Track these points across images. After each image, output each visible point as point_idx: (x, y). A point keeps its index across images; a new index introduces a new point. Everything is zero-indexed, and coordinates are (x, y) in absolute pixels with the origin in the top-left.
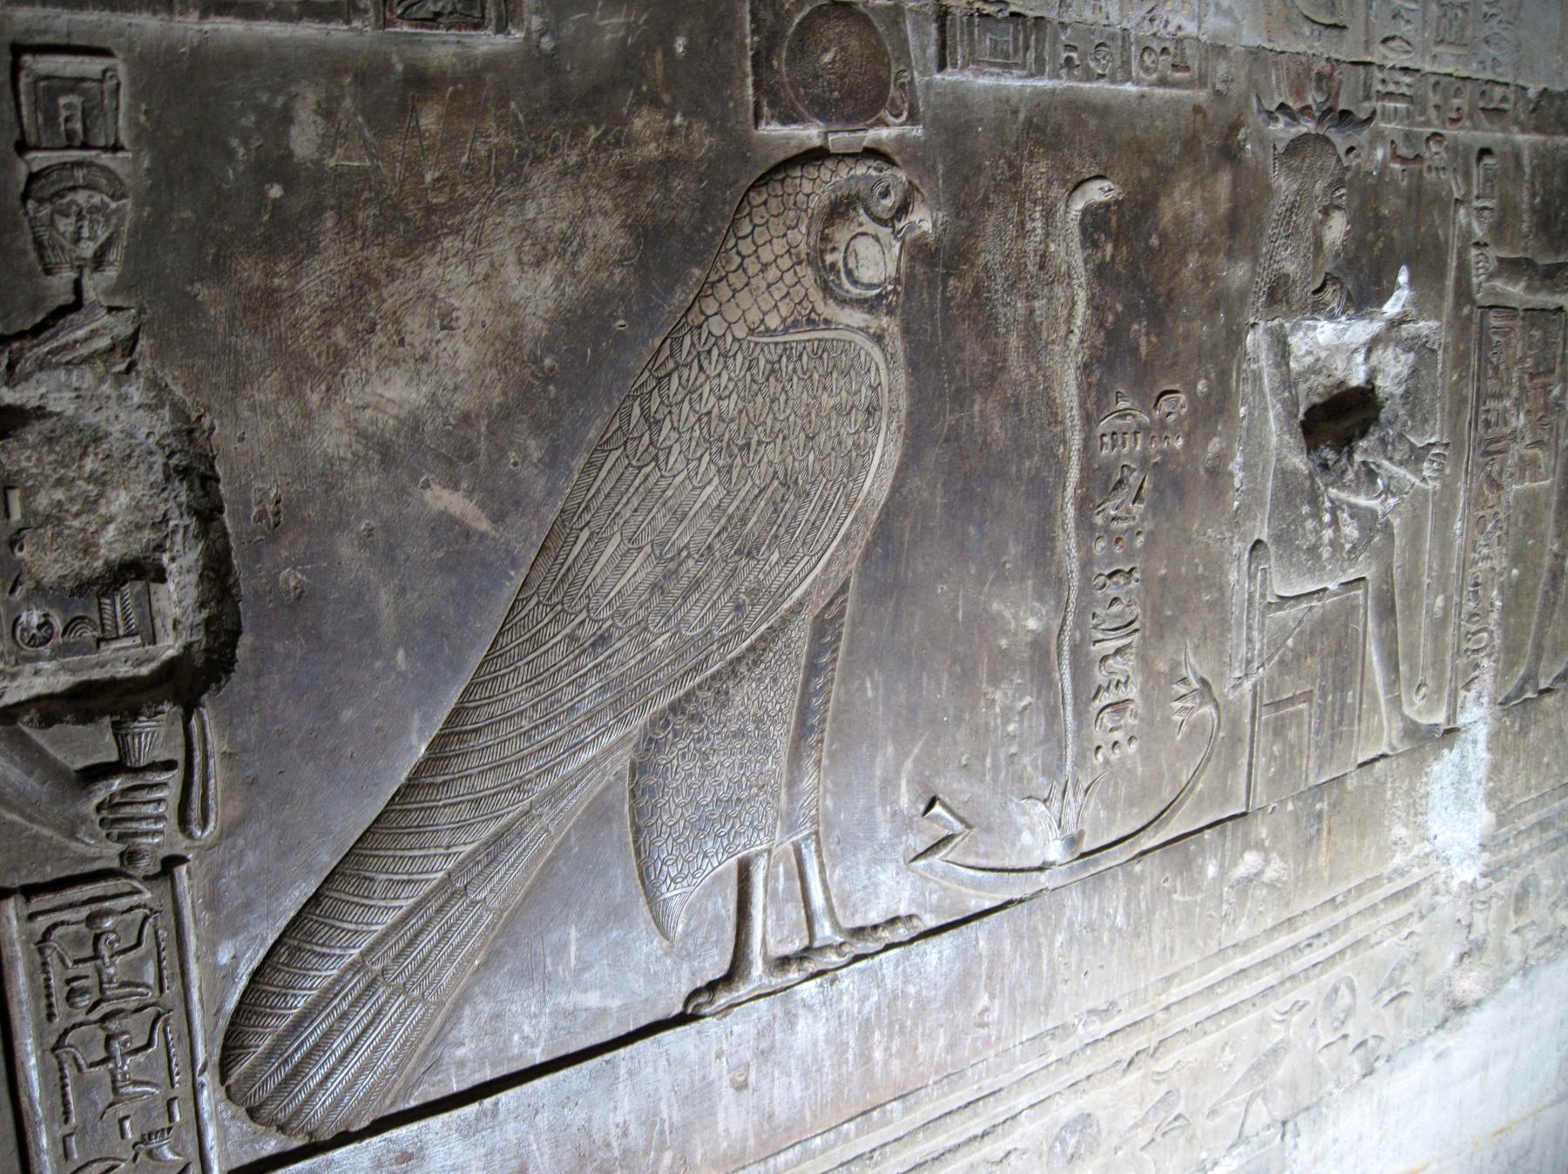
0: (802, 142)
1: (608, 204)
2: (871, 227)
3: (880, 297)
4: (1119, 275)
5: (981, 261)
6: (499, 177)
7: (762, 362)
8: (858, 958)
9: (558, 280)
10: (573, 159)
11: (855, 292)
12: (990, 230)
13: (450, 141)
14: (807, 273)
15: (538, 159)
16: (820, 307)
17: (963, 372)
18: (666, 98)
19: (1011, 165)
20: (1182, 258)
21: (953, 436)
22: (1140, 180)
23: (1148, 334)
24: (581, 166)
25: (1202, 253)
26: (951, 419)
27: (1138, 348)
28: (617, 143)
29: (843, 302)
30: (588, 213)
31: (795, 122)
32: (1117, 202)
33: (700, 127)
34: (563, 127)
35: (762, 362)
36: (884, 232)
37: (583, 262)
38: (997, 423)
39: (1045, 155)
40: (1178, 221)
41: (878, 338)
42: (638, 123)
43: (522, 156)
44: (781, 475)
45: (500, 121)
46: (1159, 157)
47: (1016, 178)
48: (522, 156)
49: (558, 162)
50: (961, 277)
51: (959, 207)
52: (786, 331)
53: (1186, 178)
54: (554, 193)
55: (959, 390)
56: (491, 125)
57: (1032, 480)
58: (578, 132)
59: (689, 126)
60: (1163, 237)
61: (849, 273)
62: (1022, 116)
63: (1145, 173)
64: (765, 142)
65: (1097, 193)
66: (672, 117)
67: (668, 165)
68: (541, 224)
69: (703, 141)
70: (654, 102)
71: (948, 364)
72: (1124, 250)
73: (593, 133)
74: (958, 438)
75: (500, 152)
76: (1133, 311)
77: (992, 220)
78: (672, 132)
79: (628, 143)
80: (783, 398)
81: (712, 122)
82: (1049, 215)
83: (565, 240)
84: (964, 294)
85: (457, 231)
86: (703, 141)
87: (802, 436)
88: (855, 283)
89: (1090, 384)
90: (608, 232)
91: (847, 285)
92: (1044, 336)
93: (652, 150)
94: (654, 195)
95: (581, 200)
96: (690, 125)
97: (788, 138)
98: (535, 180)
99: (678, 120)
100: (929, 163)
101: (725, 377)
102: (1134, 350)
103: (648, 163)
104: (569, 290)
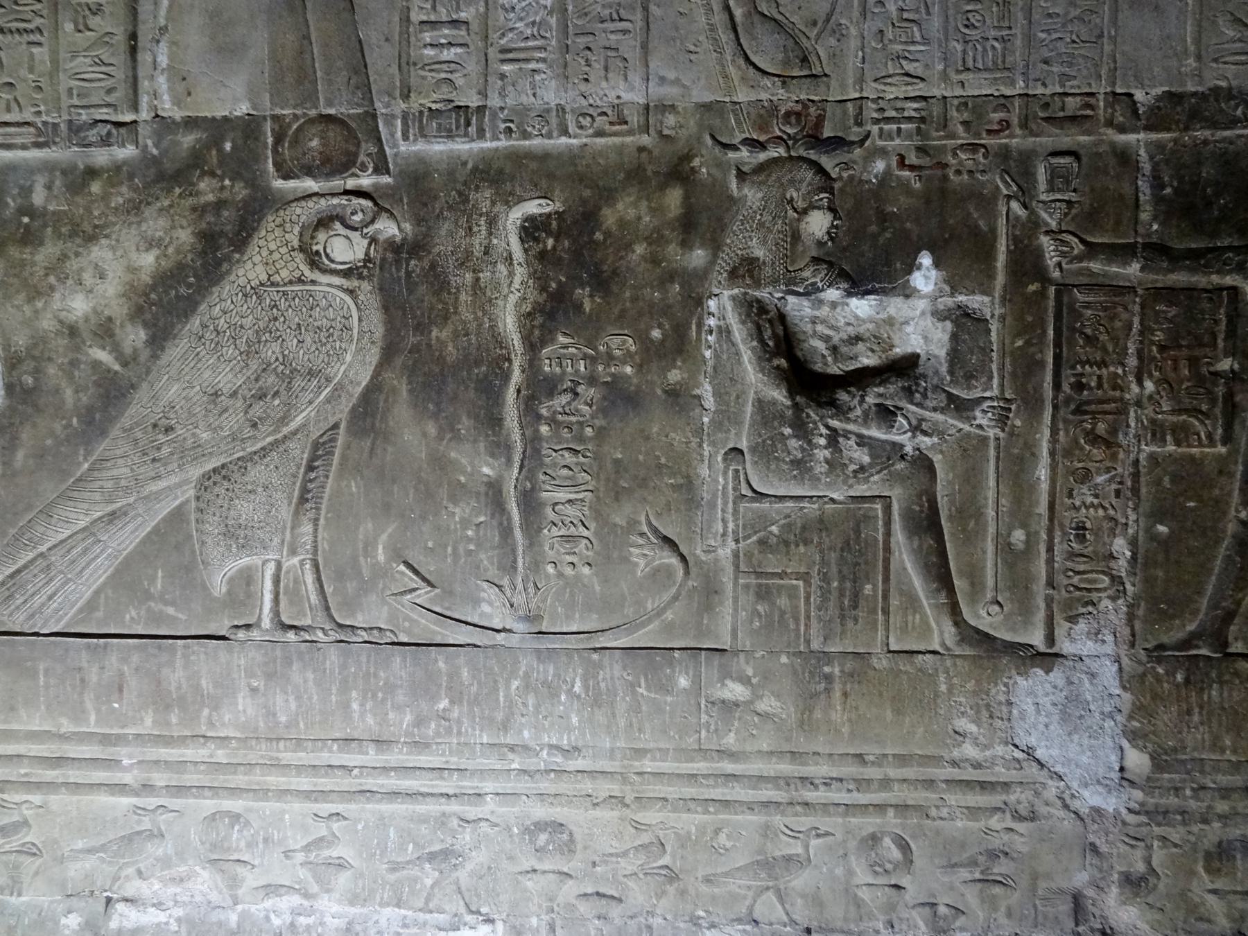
0: (306, 190)
1: (185, 223)
2: (343, 231)
3: (350, 269)
4: (560, 259)
5: (436, 250)
6: (128, 212)
7: (268, 301)
8: (342, 641)
9: (157, 258)
10: (166, 203)
11: (333, 266)
12: (443, 232)
13: (105, 197)
14: (299, 257)
15: (148, 204)
16: (307, 273)
17: (423, 314)
18: (219, 172)
19: (460, 194)
20: (629, 247)
21: (415, 349)
22: (581, 197)
23: (591, 296)
24: (171, 206)
25: (650, 244)
26: (412, 340)
27: (582, 304)
28: (191, 195)
29: (325, 271)
30: (173, 227)
31: (293, 178)
32: (557, 213)
33: (239, 185)
34: (162, 190)
35: (268, 301)
36: (355, 236)
37: (170, 250)
38: (450, 344)
39: (490, 187)
40: (622, 223)
41: (351, 292)
42: (202, 185)
43: (140, 202)
44: (281, 359)
45: (129, 187)
46: (601, 184)
47: (466, 200)
48: (140, 202)
49: (159, 205)
50: (420, 259)
51: (418, 221)
52: (285, 285)
53: (629, 195)
54: (156, 219)
55: (419, 324)
56: (124, 189)
57: (479, 381)
58: (169, 191)
59: (233, 186)
60: (608, 234)
61: (327, 256)
62: (470, 166)
63: (587, 193)
64: (280, 190)
65: (533, 207)
66: (222, 180)
67: (220, 205)
68: (149, 233)
69: (241, 192)
70: (212, 174)
71: (411, 308)
72: (566, 243)
73: (177, 191)
74: (418, 351)
75: (129, 201)
76: (576, 281)
77: (445, 227)
78: (223, 188)
79: (197, 195)
80: (282, 319)
81: (246, 182)
82: (492, 222)
83: (161, 239)
84: (423, 269)
85: (106, 236)
86: (241, 192)
87: (295, 341)
88: (332, 261)
89: (533, 327)
90: (185, 236)
91: (326, 262)
92: (489, 293)
93: (210, 197)
94: (210, 218)
95: (170, 222)
96: (233, 186)
97: (295, 189)
98: (147, 214)
99: (227, 182)
100: (397, 197)
101: (245, 307)
102: (579, 307)
103: (207, 204)
104: (163, 263)
